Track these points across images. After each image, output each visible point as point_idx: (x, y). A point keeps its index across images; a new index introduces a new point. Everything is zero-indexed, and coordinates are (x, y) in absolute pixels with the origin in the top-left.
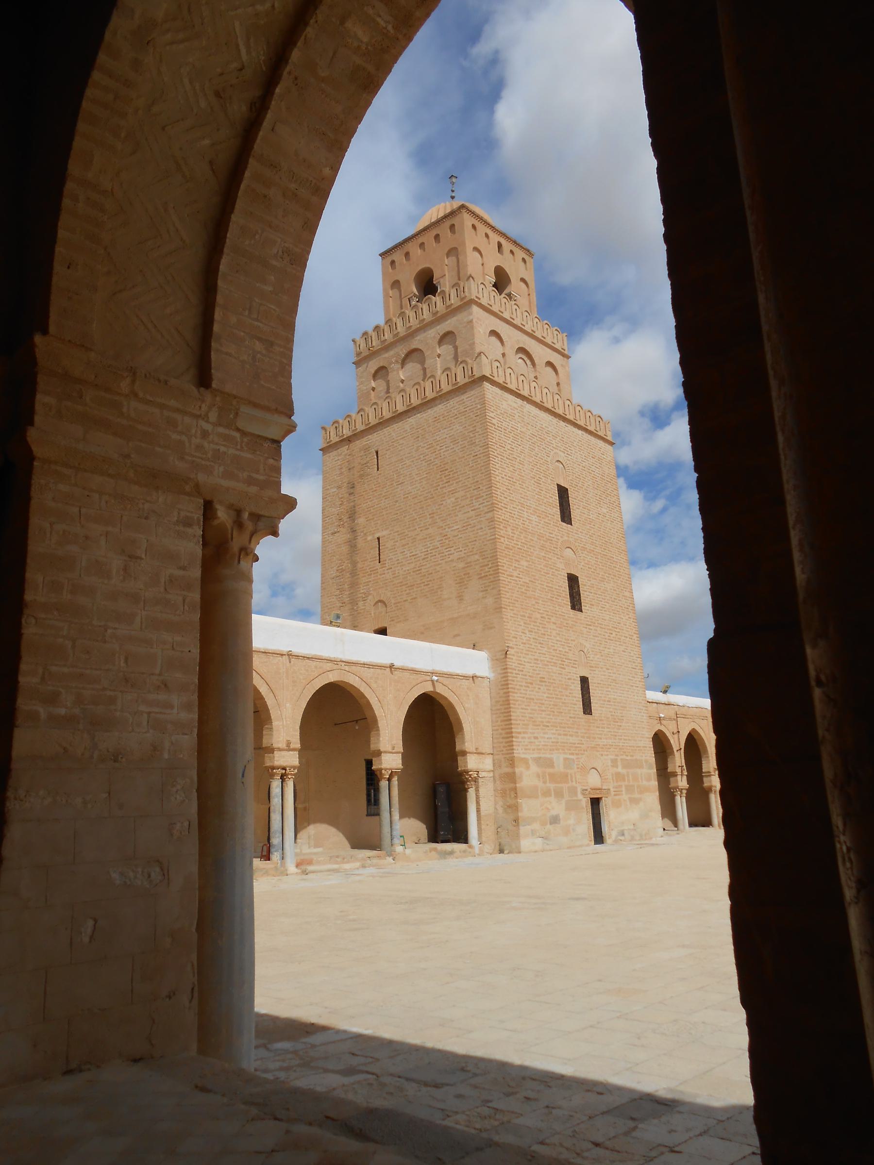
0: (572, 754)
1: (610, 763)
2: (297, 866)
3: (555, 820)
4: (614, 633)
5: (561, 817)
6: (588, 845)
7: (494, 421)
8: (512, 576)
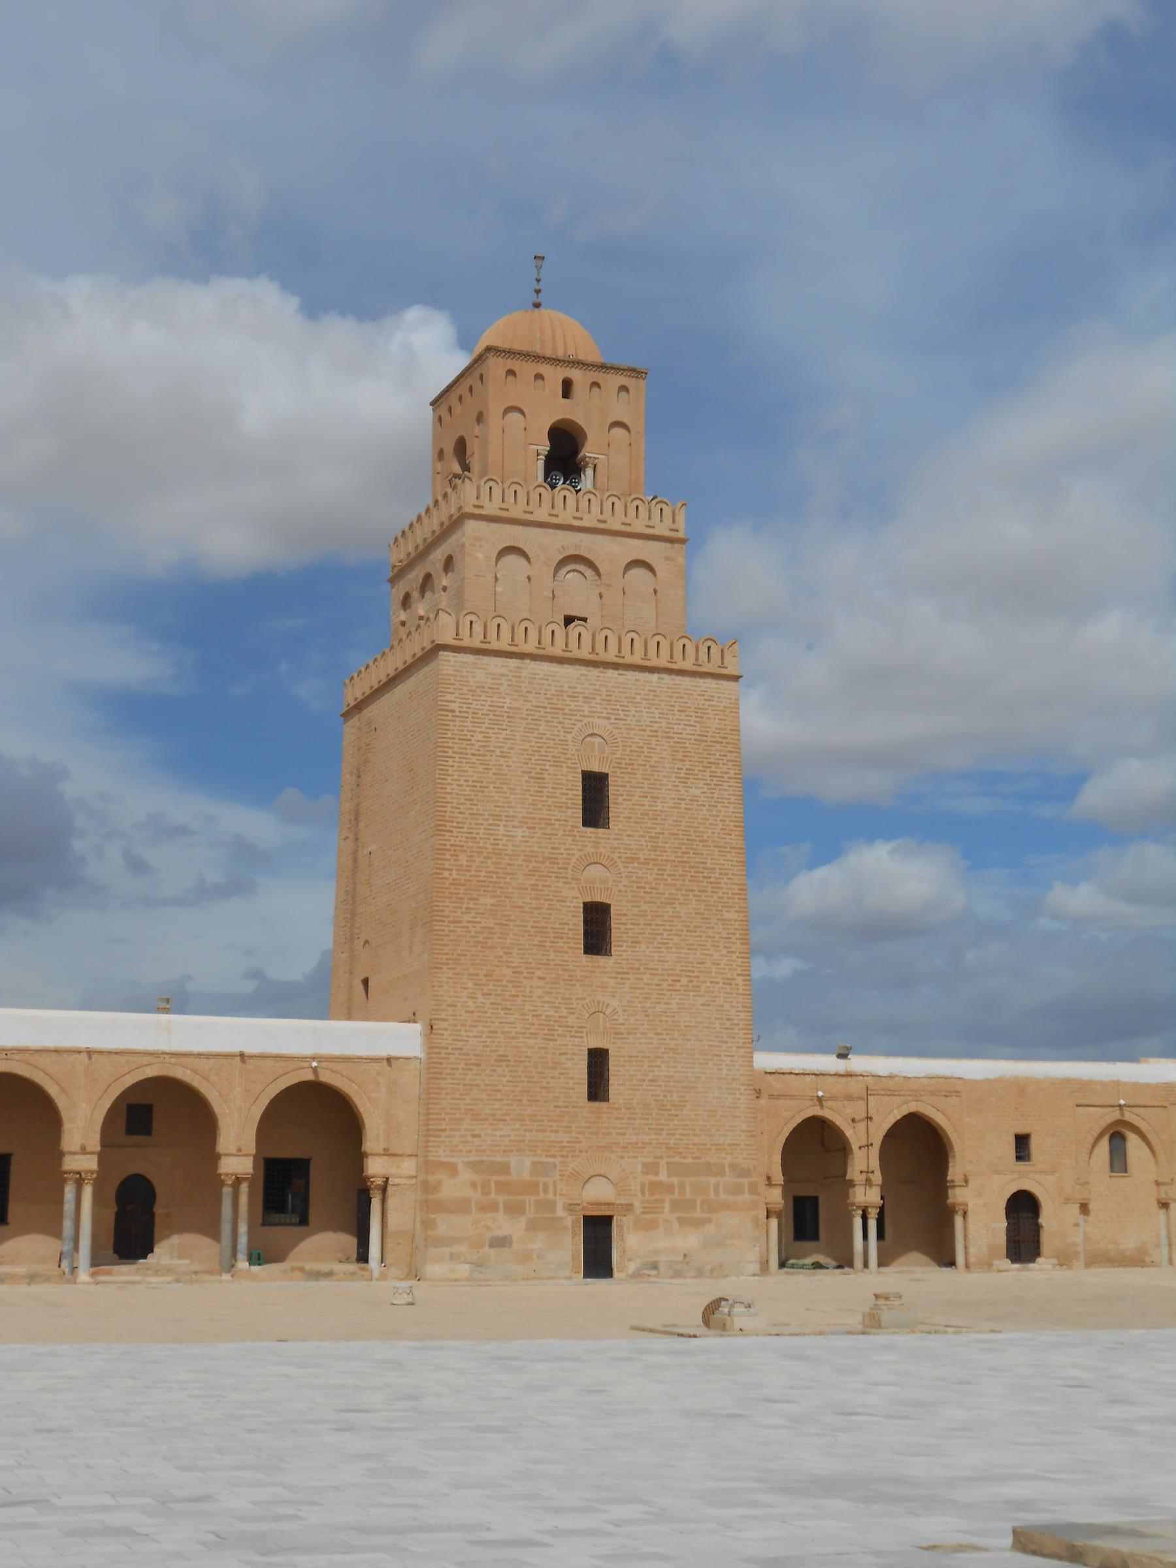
0: (554, 1156)
1: (639, 1169)
2: (93, 1275)
3: (501, 1242)
4: (684, 981)
5: (514, 1239)
6: (570, 1278)
7: (452, 706)
8: (459, 922)
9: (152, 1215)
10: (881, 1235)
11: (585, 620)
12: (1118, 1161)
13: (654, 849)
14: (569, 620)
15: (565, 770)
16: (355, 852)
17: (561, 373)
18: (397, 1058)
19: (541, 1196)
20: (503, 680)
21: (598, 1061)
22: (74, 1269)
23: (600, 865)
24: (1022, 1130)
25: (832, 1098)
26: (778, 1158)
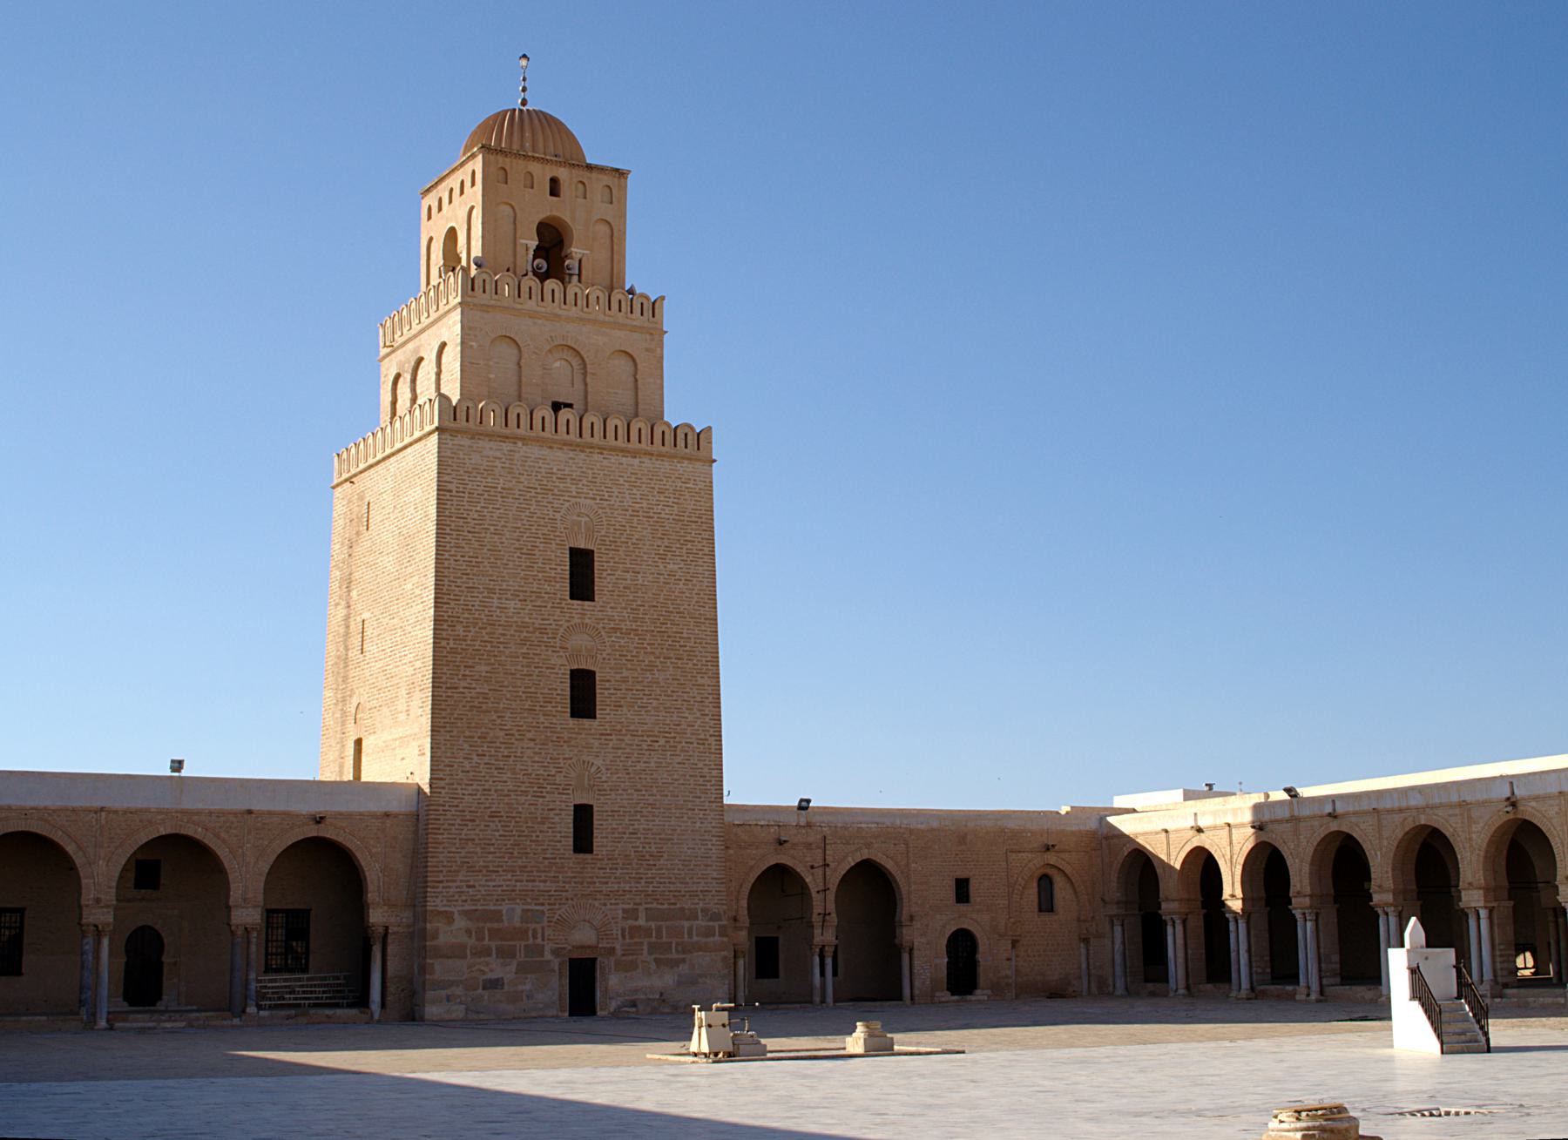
3: (494, 984)
4: (662, 742)
7: (449, 486)
9: (161, 964)
10: (835, 974)
11: (570, 406)
12: (1046, 903)
13: (635, 620)
14: (557, 407)
15: (554, 546)
16: (347, 618)
17: (550, 171)
18: (396, 816)
20: (497, 463)
21: (583, 814)
22: (93, 1016)
23: (584, 634)
24: (962, 875)
26: (744, 903)
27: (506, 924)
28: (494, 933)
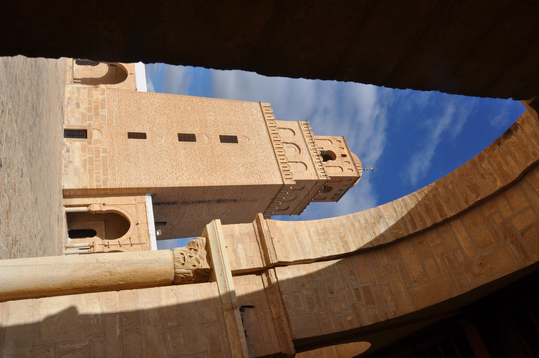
3: (78, 105)
13: (218, 156)
17: (347, 154)
19: (94, 117)
21: (142, 136)
23: (207, 141)
25: (138, 229)
26: (112, 208)
27: (100, 110)
28: (97, 107)
